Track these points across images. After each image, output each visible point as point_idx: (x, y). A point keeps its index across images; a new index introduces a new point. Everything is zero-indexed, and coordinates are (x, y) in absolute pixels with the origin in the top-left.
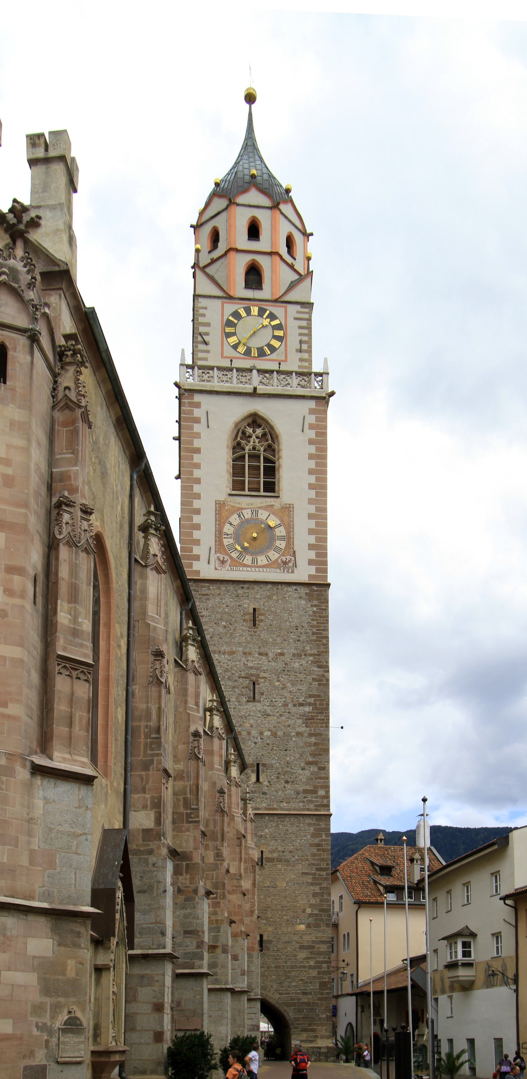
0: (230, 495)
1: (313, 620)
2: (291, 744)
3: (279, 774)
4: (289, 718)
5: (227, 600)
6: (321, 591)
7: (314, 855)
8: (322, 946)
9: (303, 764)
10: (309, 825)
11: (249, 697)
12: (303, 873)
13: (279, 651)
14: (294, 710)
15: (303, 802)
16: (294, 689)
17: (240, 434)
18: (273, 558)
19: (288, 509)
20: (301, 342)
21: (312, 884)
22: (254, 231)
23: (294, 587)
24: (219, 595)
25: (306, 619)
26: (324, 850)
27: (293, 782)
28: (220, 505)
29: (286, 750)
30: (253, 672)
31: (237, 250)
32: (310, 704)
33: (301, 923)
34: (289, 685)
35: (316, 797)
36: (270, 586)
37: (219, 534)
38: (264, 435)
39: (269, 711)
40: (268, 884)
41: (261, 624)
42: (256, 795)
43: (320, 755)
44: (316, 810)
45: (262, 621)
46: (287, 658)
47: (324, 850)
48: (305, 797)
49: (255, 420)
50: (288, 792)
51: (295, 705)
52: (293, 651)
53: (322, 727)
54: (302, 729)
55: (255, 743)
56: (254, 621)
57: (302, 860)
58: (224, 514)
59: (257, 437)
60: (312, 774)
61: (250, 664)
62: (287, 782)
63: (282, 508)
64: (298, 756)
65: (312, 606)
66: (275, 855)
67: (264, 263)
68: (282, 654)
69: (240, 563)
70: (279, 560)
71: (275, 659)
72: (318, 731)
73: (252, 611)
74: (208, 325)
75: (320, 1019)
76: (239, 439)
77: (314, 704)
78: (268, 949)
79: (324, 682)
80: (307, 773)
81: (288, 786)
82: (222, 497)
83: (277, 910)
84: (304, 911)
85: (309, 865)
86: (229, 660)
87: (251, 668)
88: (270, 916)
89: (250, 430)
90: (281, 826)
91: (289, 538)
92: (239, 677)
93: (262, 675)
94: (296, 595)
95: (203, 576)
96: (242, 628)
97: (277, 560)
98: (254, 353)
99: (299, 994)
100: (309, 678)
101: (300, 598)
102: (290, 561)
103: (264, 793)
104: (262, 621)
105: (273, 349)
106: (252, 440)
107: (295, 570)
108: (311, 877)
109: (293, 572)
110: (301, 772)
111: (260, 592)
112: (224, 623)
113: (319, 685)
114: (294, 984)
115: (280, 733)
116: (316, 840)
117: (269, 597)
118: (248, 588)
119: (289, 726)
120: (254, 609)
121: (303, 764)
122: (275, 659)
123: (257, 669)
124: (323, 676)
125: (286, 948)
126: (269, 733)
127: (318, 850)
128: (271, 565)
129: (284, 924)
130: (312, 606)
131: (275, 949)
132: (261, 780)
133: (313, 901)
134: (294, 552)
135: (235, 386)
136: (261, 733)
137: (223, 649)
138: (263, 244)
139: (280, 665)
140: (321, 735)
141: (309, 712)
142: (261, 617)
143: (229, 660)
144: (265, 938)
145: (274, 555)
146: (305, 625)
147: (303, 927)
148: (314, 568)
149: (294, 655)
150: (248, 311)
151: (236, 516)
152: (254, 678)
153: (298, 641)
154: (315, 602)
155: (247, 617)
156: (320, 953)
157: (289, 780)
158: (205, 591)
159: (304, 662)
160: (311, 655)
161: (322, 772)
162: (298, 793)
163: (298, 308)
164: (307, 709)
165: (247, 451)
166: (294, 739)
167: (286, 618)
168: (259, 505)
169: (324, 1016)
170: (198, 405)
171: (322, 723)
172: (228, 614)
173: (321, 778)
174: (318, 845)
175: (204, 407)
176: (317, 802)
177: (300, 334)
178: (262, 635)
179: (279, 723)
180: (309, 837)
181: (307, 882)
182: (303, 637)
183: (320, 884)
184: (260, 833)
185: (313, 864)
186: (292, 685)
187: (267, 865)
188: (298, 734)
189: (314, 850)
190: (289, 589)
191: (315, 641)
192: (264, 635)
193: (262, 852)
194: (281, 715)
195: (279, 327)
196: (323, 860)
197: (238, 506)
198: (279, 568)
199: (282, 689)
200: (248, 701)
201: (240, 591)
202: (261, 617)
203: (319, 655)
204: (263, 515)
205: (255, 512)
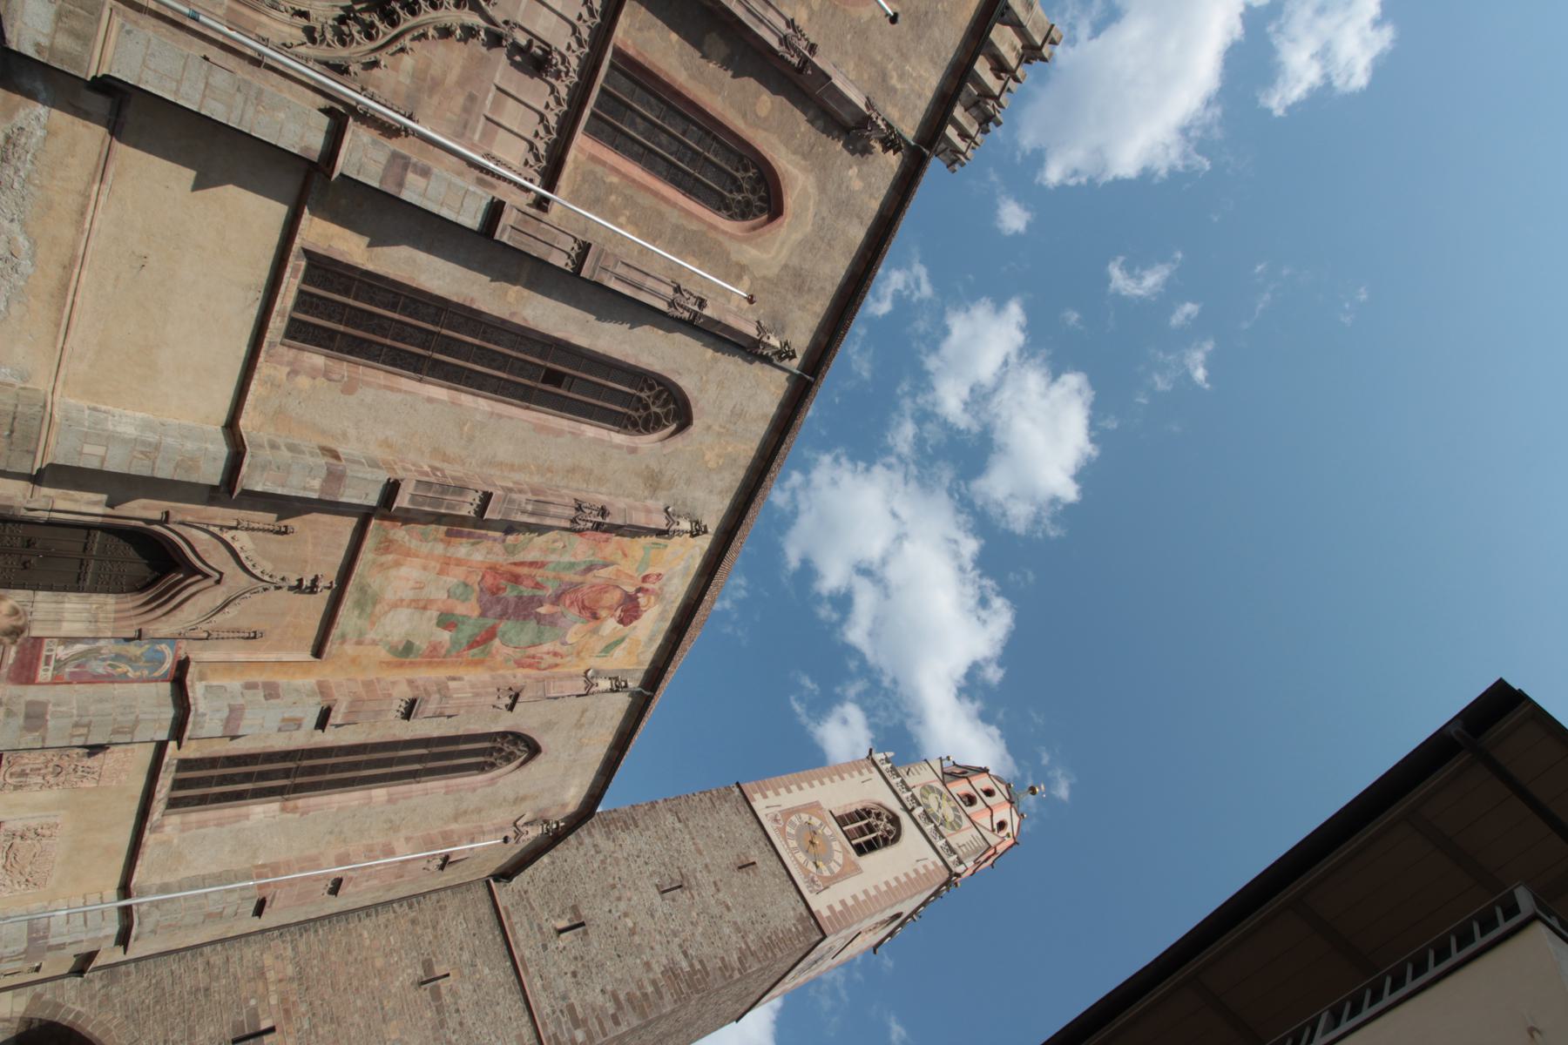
2: (630, 961)
9: (609, 988)
14: (674, 947)
16: (699, 938)
19: (857, 870)
22: (989, 793)
32: (691, 965)
34: (700, 929)
38: (889, 832)
39: (657, 915)
40: (388, 1005)
49: (894, 820)
50: (560, 982)
51: (680, 946)
52: (739, 920)
54: (658, 969)
60: (601, 1008)
62: (574, 974)
64: (618, 976)
66: (447, 999)
68: (728, 909)
71: (719, 902)
72: (664, 990)
80: (600, 999)
88: (320, 1031)
90: (501, 991)
91: (835, 878)
93: (695, 893)
95: (754, 804)
100: (721, 953)
103: (545, 947)
110: (598, 990)
115: (637, 939)
117: (774, 875)
121: (609, 988)
122: (719, 902)
126: (630, 924)
132: (563, 936)
136: (626, 915)
139: (716, 911)
140: (661, 998)
146: (772, 924)
159: (734, 938)
162: (564, 997)
164: (684, 964)
173: (601, 1024)
182: (759, 928)
184: (479, 962)
187: (425, 993)
188: (647, 965)
192: (736, 881)
201: (761, 844)
204: (836, 846)
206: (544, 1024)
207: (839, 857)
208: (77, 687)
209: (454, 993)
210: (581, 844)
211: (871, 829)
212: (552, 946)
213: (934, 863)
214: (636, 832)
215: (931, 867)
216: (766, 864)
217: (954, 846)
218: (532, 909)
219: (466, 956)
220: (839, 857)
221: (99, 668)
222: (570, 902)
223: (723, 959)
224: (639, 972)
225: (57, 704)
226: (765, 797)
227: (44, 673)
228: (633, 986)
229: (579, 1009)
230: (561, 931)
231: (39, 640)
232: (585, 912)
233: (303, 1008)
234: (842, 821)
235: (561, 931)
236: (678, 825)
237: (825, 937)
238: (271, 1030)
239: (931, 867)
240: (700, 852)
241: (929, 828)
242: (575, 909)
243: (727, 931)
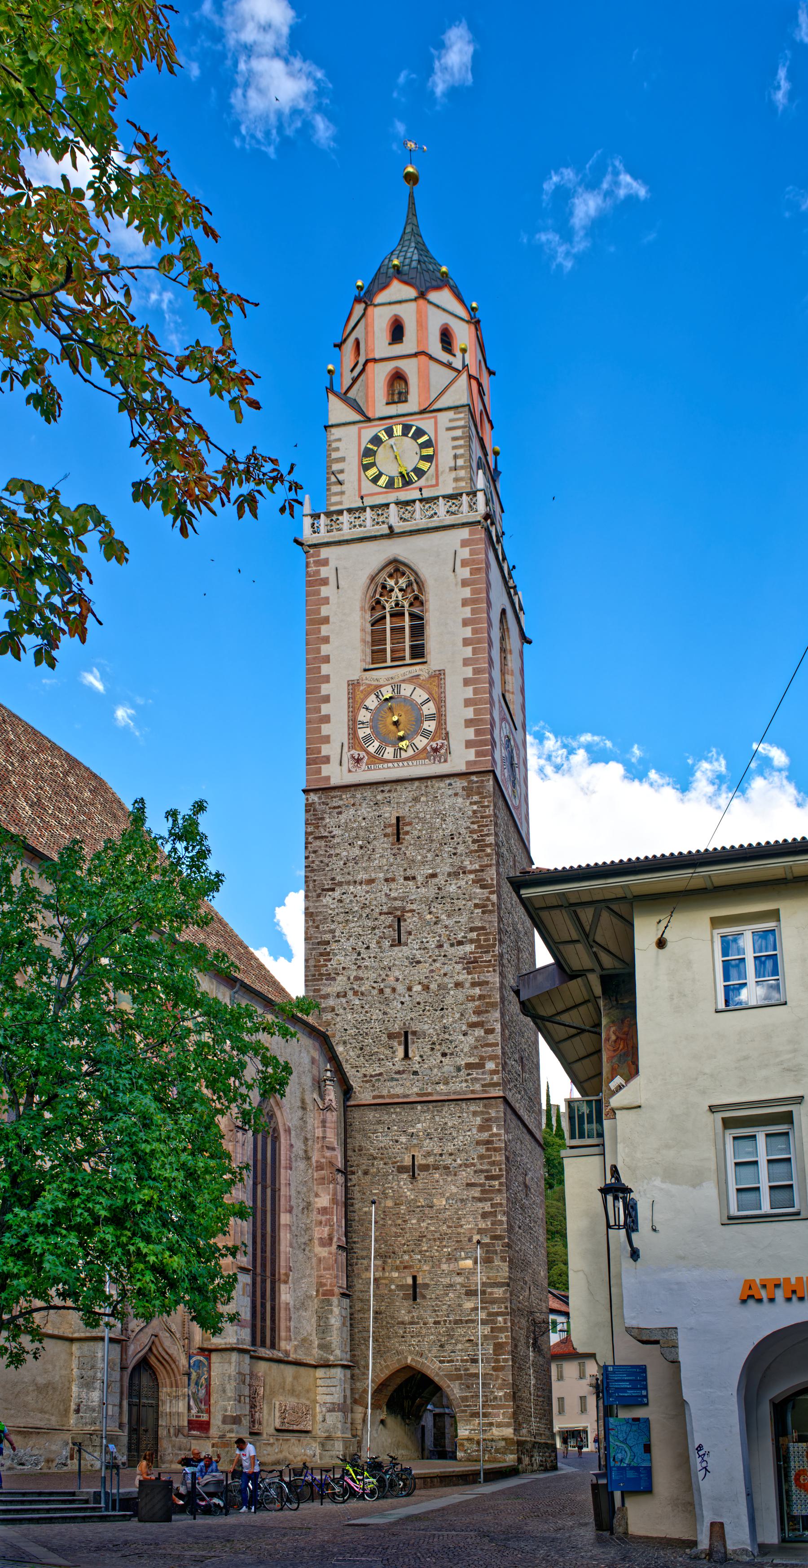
0: (365, 670)
1: (473, 823)
2: (449, 1000)
3: (434, 1043)
4: (444, 964)
5: (364, 811)
6: (482, 781)
7: (481, 1157)
8: (495, 1290)
9: (464, 1028)
10: (475, 1114)
11: (393, 940)
12: (468, 1185)
13: (430, 871)
14: (451, 951)
15: (466, 1081)
16: (450, 922)
17: (379, 590)
18: (420, 746)
20: (456, 457)
21: (480, 1200)
22: (397, 332)
23: (448, 782)
24: (353, 805)
25: (464, 823)
26: (495, 1150)
27: (452, 1054)
28: (353, 685)
29: (442, 1009)
30: (398, 904)
31: (375, 361)
32: (472, 941)
33: (466, 1258)
34: (444, 917)
35: (483, 1073)
36: (417, 784)
37: (353, 724)
38: (410, 584)
41: (407, 837)
42: (404, 1076)
43: (487, 1012)
44: (485, 1092)
45: (407, 833)
46: (440, 880)
47: (495, 1150)
48: (469, 1075)
49: (397, 567)
50: (446, 1069)
51: (452, 945)
52: (448, 869)
53: (488, 972)
54: (463, 977)
55: (402, 1003)
56: (398, 834)
57: (466, 1166)
58: (359, 696)
59: (401, 590)
60: (477, 1040)
61: (393, 894)
62: (444, 1055)
63: (430, 677)
64: (458, 1015)
65: (471, 803)
66: (431, 1160)
67: (409, 368)
68: (434, 876)
69: (379, 759)
70: (428, 748)
71: (425, 884)
72: (483, 978)
73: (394, 821)
74: (342, 459)
75: (495, 1398)
76: (377, 596)
77: (478, 940)
78: (424, 1297)
79: (490, 908)
80: (471, 1040)
81: (446, 1060)
82: (356, 674)
83: (435, 1240)
84: (470, 1240)
85: (475, 1172)
86: (367, 892)
87: (395, 899)
89: (391, 582)
90: (437, 1118)
91: (440, 717)
92: (381, 914)
94: (450, 792)
96: (382, 845)
97: (425, 748)
98: (399, 483)
99: (466, 1361)
101: (456, 795)
102: (441, 747)
103: (415, 1073)
104: (407, 833)
105: (420, 473)
106: (393, 594)
107: (449, 759)
108: (479, 1189)
109: (445, 761)
110: (461, 1037)
111: (405, 794)
112: (360, 843)
113: (483, 912)
114: (459, 1347)
115: (433, 986)
116: (485, 1135)
117: (416, 800)
118: (390, 791)
119: (445, 975)
120: (398, 818)
121: (464, 1028)
123: (402, 899)
124: (488, 899)
125: (447, 1295)
127: (488, 1149)
128: (420, 755)
129: (444, 1260)
130: (471, 803)
131: (433, 1296)
132: (410, 1055)
133: (482, 1225)
134: (447, 734)
135: (370, 529)
136: (410, 989)
137: (359, 878)
138: (409, 344)
139: (431, 892)
140: (487, 983)
141: (471, 953)
142: (407, 828)
143: (367, 892)
144: (420, 1281)
145: (421, 742)
146: (463, 831)
147: (469, 1263)
148: (472, 751)
149: (449, 875)
150: (390, 432)
151: (373, 697)
152: (399, 913)
153: (455, 854)
154: (476, 798)
155: (389, 830)
156: (493, 1302)
157: (447, 1051)
158: (336, 802)
160: (471, 872)
161: (490, 1036)
162: (459, 1069)
163: (451, 414)
164: (469, 948)
165: (388, 609)
166: (452, 992)
167: (438, 825)
168: (401, 678)
169: (501, 1394)
170: (325, 562)
171: (488, 967)
172: (366, 829)
174: (488, 1142)
175: (332, 564)
176: (485, 1079)
177: (454, 448)
178: (408, 853)
179: (432, 971)
180: (475, 1131)
181: (474, 1198)
183: (491, 1199)
184: (411, 1130)
185: (482, 1171)
186: (449, 916)
187: (421, 1175)
188: (458, 985)
189: (482, 1150)
190: (442, 785)
191: (476, 851)
192: (411, 852)
193: (413, 1156)
194: (434, 961)
195: (428, 444)
196: (493, 1163)
197: (376, 683)
198: (428, 758)
199: (435, 923)
200: (392, 946)
201: (379, 797)
202: (407, 828)
203: (483, 871)
204: (406, 690)
205: (396, 687)
206: (473, 1092)
207: (420, 695)
208: (212, 1401)
209: (429, 1154)
210: (333, 1010)
211: (397, 615)
212: (416, 1067)
213: (464, 543)
214: (334, 946)
215: (465, 553)
216: (400, 804)
217: (450, 491)
218: (381, 1074)
219: (403, 1139)
220: (420, 695)
221: (202, 1393)
222: (384, 1038)
223: (476, 906)
224: (460, 994)
225: (226, 1410)
226: (327, 760)
227: (205, 1417)
228: (471, 1005)
229: (471, 1060)
230: (406, 1055)
231: (190, 1422)
232: (396, 1028)
233: (406, 1257)
234: (377, 656)
235: (406, 1055)
236: (337, 894)
237: (493, 772)
238: (414, 1278)
239: (465, 553)
240: (371, 881)
241: (419, 519)
242: (391, 1036)
243: (453, 888)
